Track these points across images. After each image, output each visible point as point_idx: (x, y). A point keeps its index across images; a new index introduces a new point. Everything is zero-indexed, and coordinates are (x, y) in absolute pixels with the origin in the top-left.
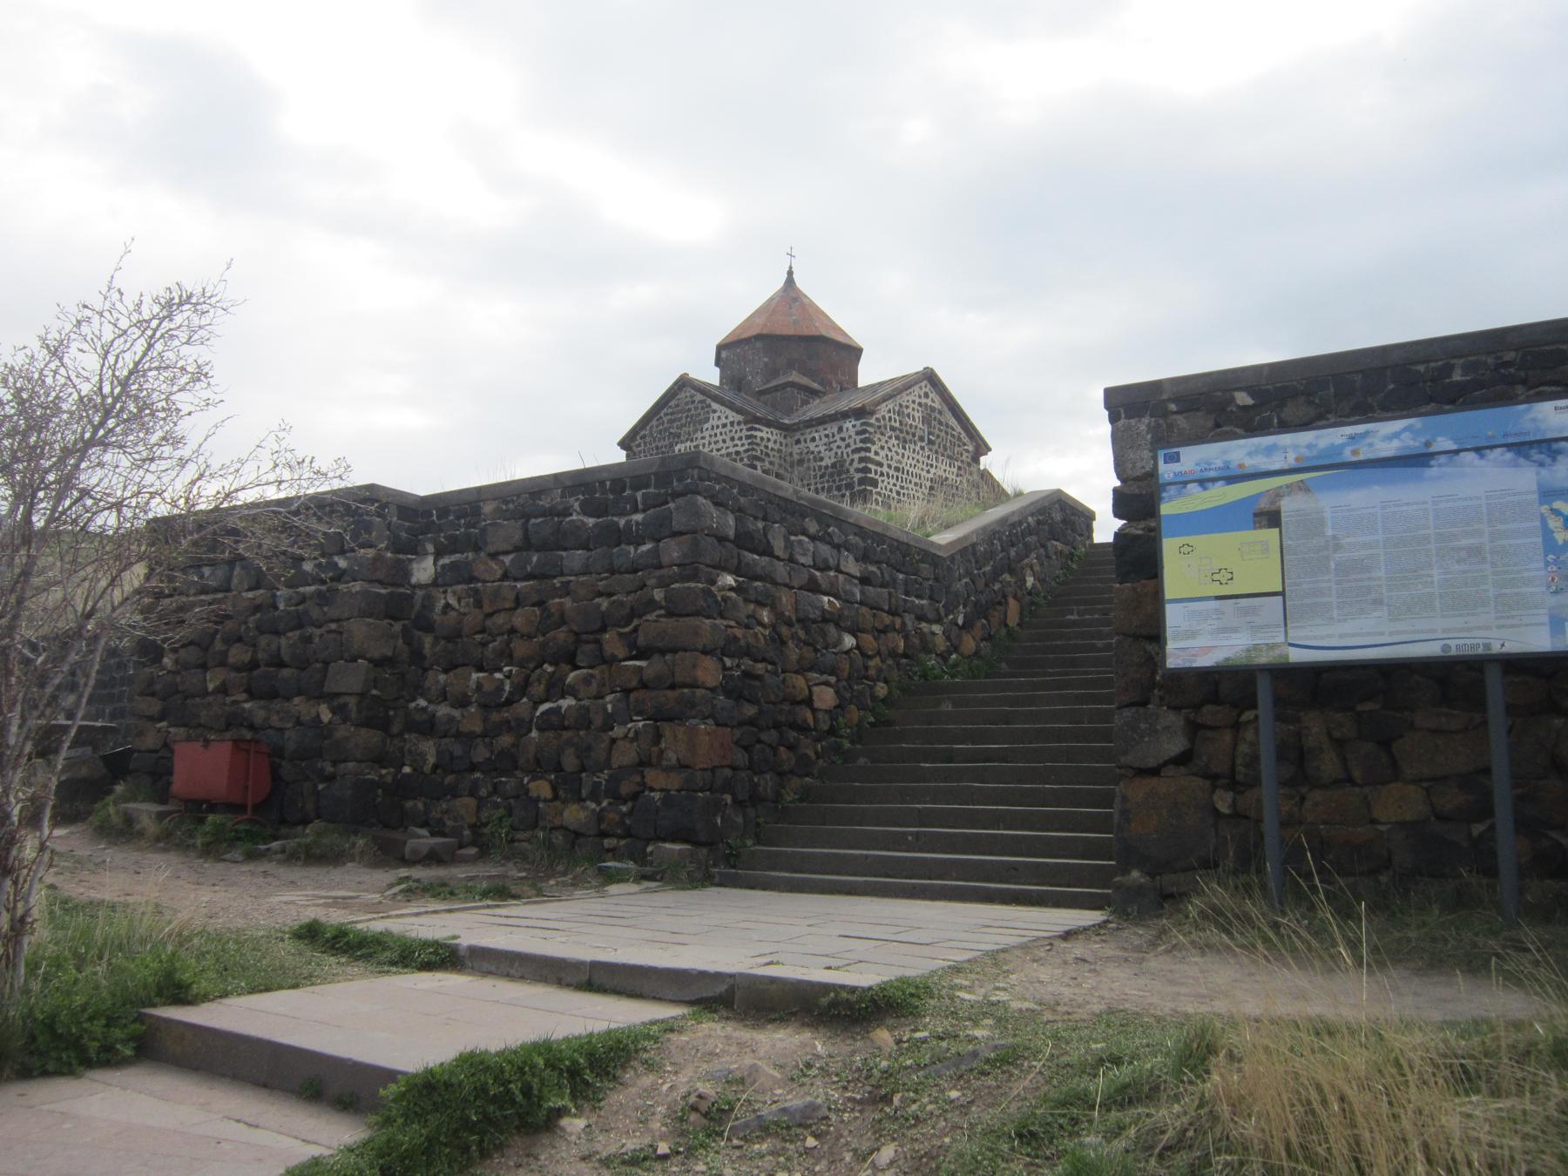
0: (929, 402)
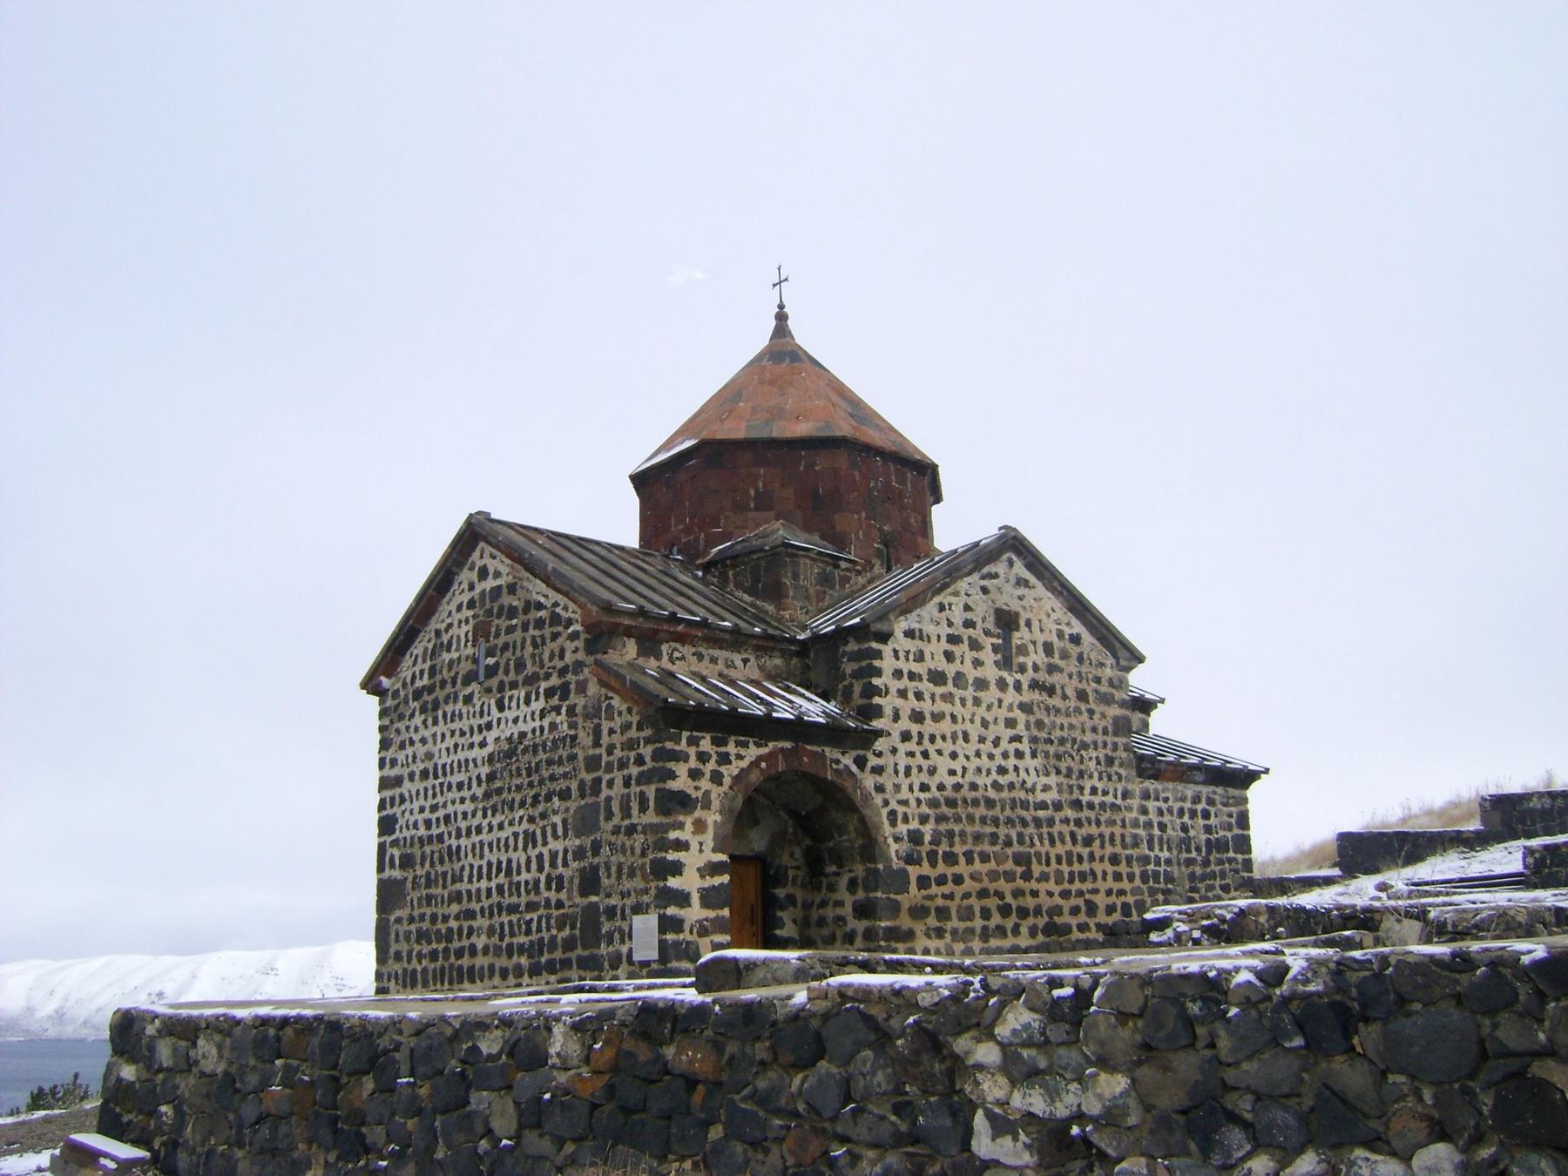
0: (490, 583)
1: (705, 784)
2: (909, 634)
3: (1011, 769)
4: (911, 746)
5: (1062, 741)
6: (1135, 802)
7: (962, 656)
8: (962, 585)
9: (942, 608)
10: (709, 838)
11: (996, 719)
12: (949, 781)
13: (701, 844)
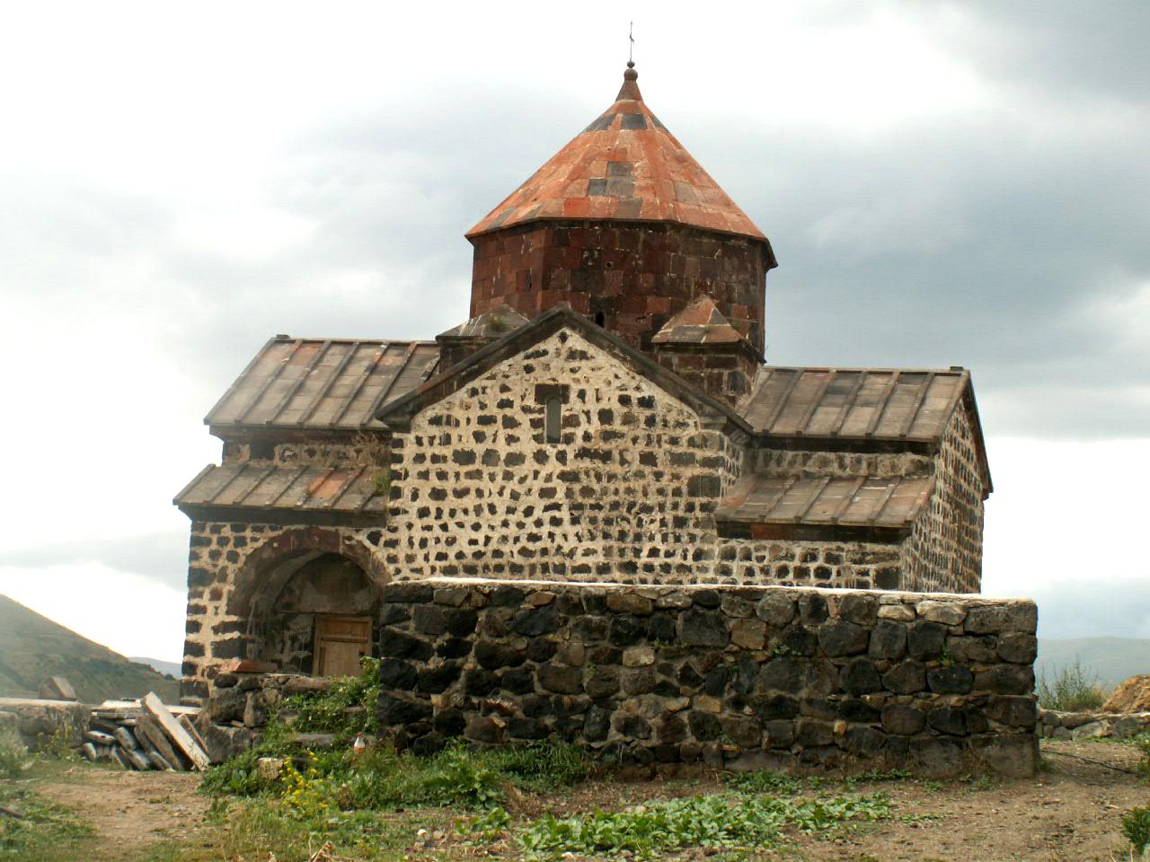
1: (222, 562)
2: (436, 421)
3: (545, 536)
4: (430, 520)
5: (615, 506)
6: (712, 564)
7: (495, 435)
8: (503, 366)
9: (474, 392)
10: (223, 604)
11: (530, 490)
12: (469, 550)
13: (217, 608)
